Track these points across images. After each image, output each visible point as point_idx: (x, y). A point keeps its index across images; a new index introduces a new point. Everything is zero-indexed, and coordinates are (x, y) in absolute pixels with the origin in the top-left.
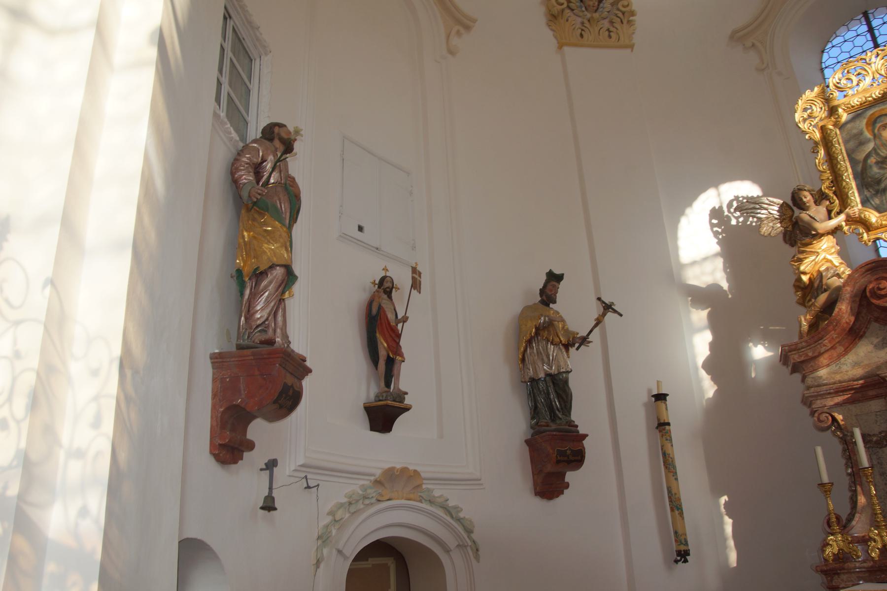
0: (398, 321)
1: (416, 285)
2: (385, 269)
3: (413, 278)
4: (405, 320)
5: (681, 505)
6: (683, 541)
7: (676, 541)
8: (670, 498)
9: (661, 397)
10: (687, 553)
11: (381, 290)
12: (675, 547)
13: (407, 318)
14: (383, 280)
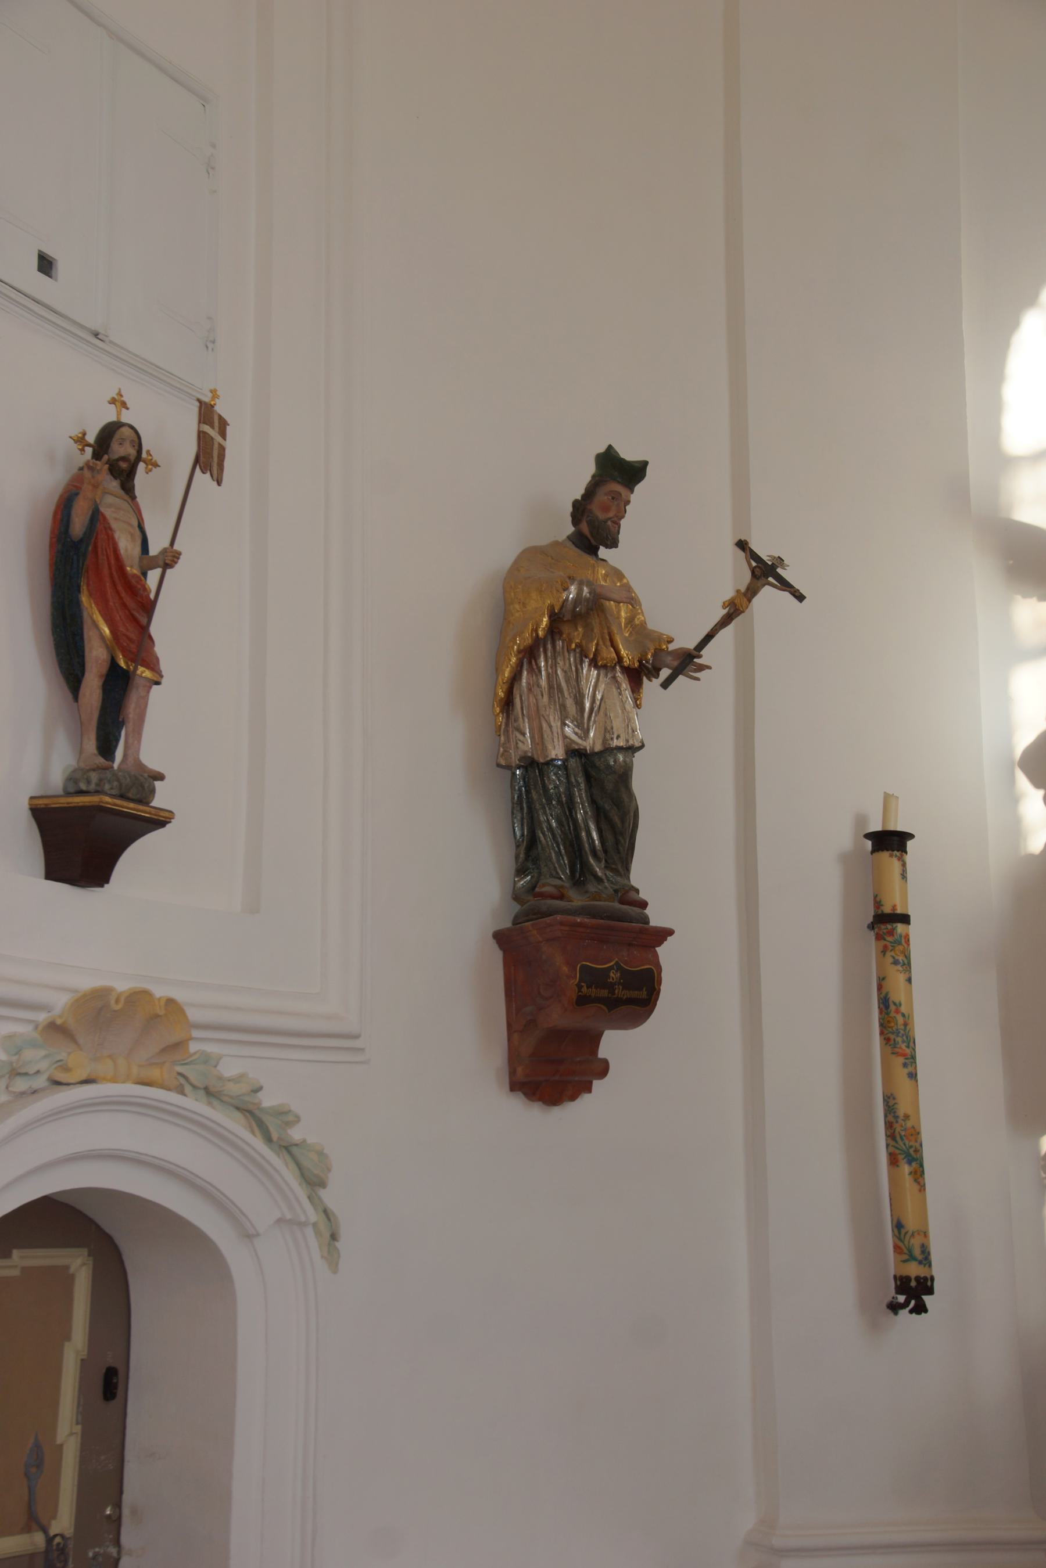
0: (147, 562)
1: (209, 458)
2: (119, 402)
3: (202, 436)
4: (169, 560)
5: (918, 1150)
6: (917, 1252)
7: (897, 1248)
8: (889, 1125)
9: (890, 842)
10: (925, 1286)
11: (102, 466)
12: (891, 1265)
14: (109, 433)
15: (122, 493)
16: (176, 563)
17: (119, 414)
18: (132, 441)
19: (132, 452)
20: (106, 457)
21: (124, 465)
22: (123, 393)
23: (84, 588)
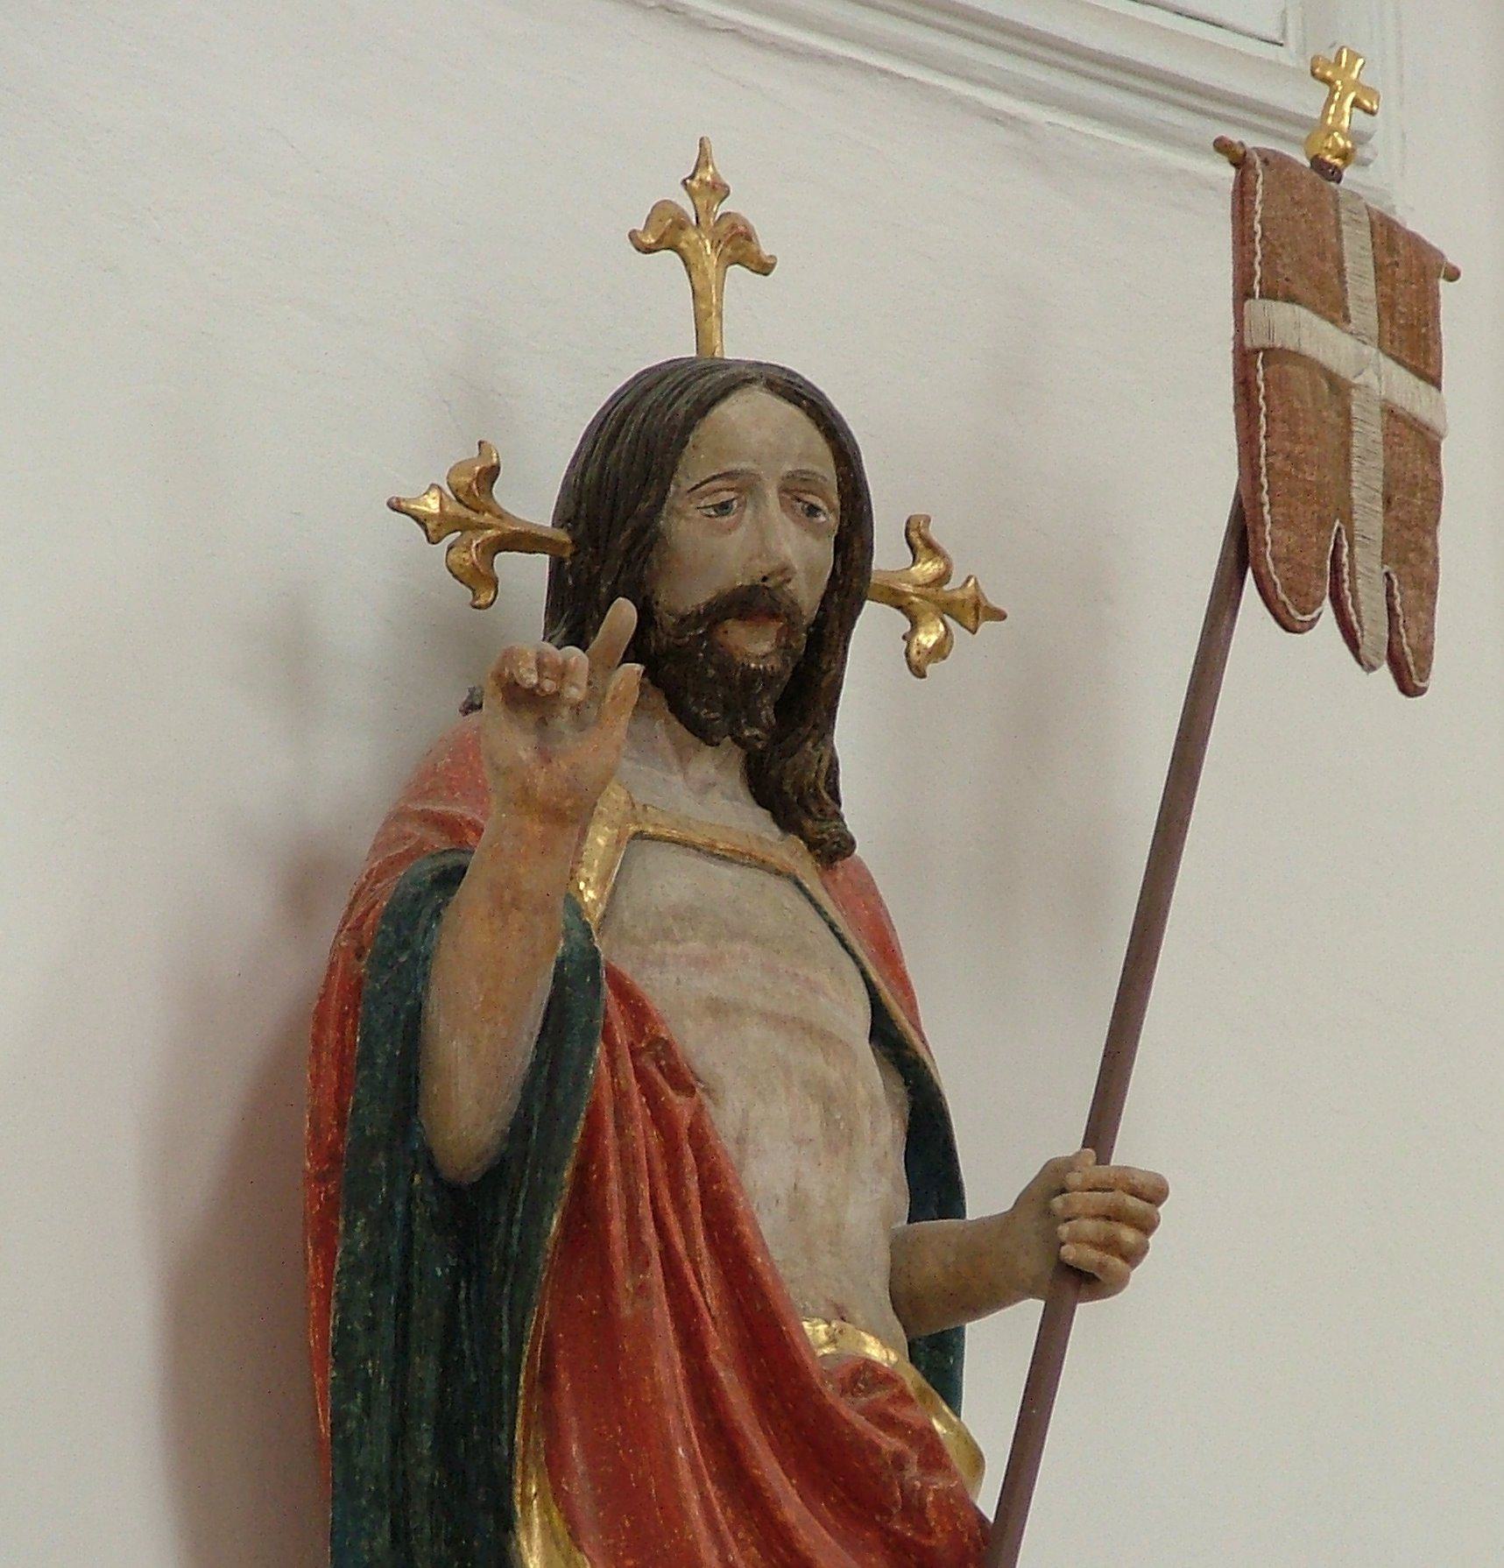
13: (1135, 1208)
15: (749, 823)
16: (1133, 1256)
17: (705, 317)
18: (795, 490)
19: (802, 553)
20: (624, 613)
21: (756, 646)
22: (722, 166)
23: (530, 1490)
